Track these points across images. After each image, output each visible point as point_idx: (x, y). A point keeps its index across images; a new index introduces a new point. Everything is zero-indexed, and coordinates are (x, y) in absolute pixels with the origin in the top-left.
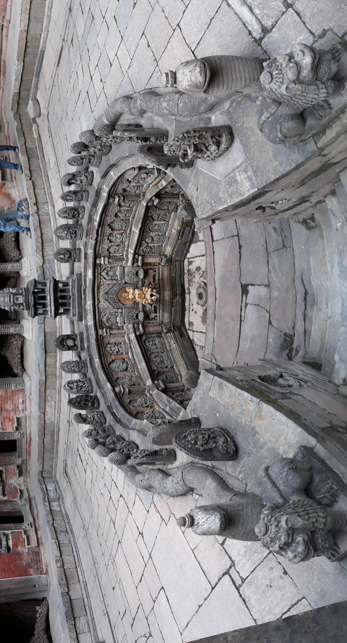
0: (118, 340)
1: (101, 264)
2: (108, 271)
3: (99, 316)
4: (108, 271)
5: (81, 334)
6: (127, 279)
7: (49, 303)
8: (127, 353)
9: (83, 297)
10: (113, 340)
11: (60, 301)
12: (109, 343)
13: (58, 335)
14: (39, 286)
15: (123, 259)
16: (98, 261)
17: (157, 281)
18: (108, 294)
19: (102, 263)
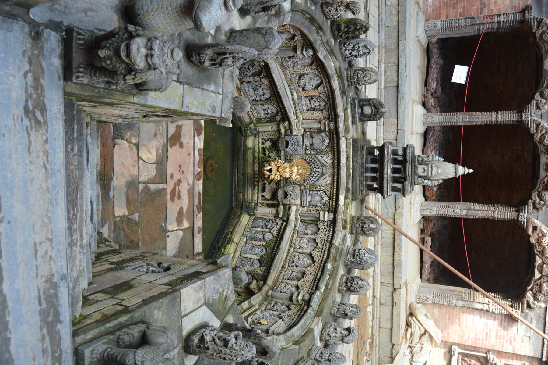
0: (310, 115)
1: (329, 212)
2: (321, 201)
3: (334, 146)
4: (321, 201)
5: (354, 123)
6: (298, 190)
7: (389, 164)
8: (299, 98)
9: (351, 170)
10: (317, 114)
13: (382, 119)
14: (399, 186)
15: (301, 216)
16: (332, 215)
17: (261, 183)
18: (322, 173)
19: (326, 213)
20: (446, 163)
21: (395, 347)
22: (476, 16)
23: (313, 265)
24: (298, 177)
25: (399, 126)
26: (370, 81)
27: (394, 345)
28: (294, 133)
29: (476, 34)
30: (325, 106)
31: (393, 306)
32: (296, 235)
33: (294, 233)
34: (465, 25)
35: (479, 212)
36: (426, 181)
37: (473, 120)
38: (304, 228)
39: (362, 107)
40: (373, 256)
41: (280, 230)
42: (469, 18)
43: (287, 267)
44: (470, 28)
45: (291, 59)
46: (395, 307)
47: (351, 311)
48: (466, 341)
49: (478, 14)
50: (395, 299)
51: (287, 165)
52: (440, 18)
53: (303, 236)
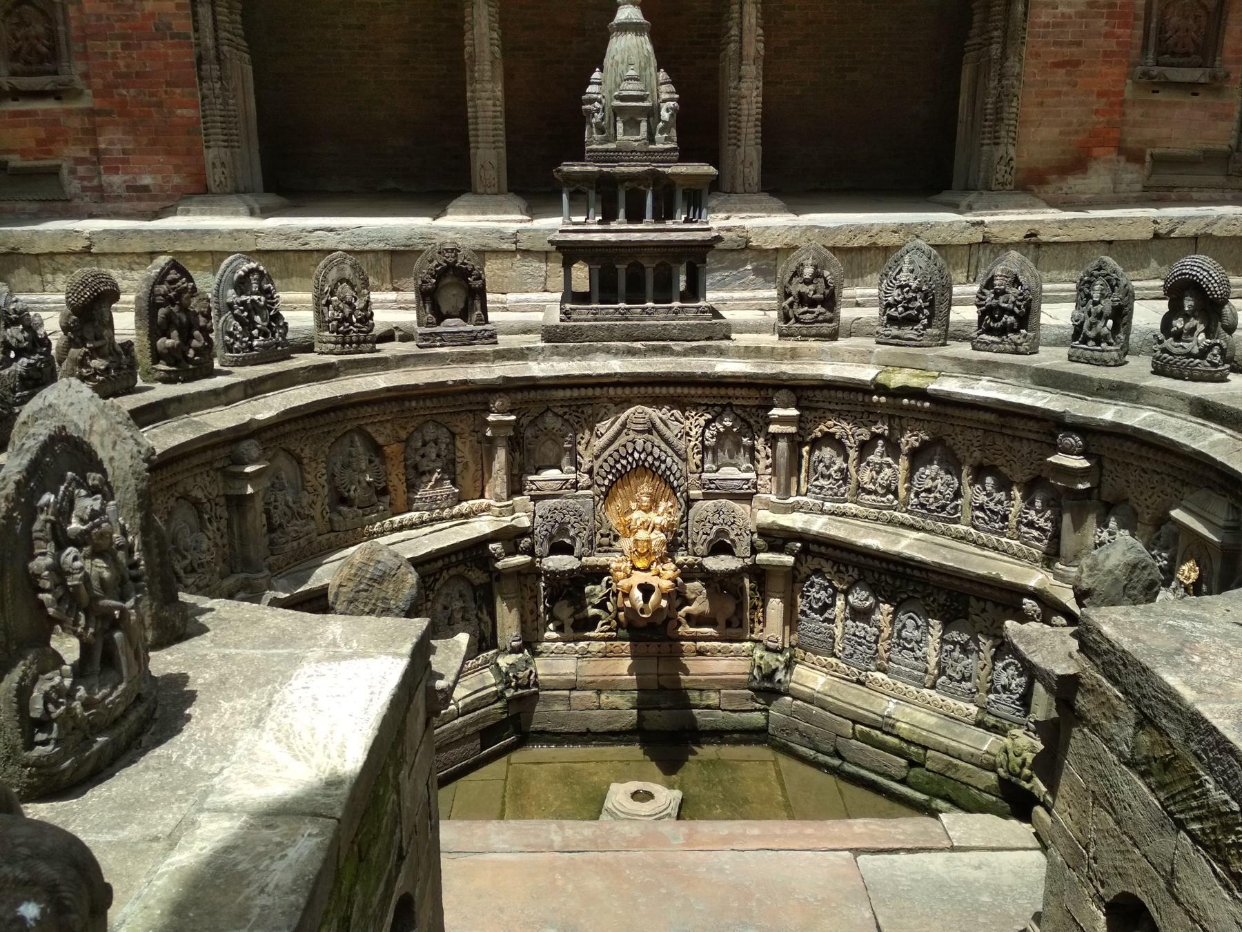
9: (638, 345)
11: (622, 268)
12: (453, 435)
15: (787, 494)
16: (783, 395)
19: (776, 412)
20: (607, 62)
21: (1163, 231)
22: (195, 50)
23: (949, 441)
24: (663, 505)
25: (505, 246)
26: (358, 282)
27: (1157, 236)
28: (525, 522)
29: (247, 56)
30: (438, 425)
31: (1039, 245)
32: (850, 507)
33: (844, 514)
34: (220, 79)
35: (746, 23)
36: (665, 115)
37: (487, 51)
38: (822, 482)
39: (440, 318)
40: (907, 258)
41: (836, 562)
42: (199, 69)
43: (961, 527)
44: (228, 66)
45: (277, 520)
46: (1043, 238)
47: (1103, 296)
48: (1118, 44)
49: (191, 46)
50: (1016, 239)
51: (626, 544)
52: (202, 154)
53: (853, 485)
